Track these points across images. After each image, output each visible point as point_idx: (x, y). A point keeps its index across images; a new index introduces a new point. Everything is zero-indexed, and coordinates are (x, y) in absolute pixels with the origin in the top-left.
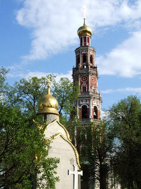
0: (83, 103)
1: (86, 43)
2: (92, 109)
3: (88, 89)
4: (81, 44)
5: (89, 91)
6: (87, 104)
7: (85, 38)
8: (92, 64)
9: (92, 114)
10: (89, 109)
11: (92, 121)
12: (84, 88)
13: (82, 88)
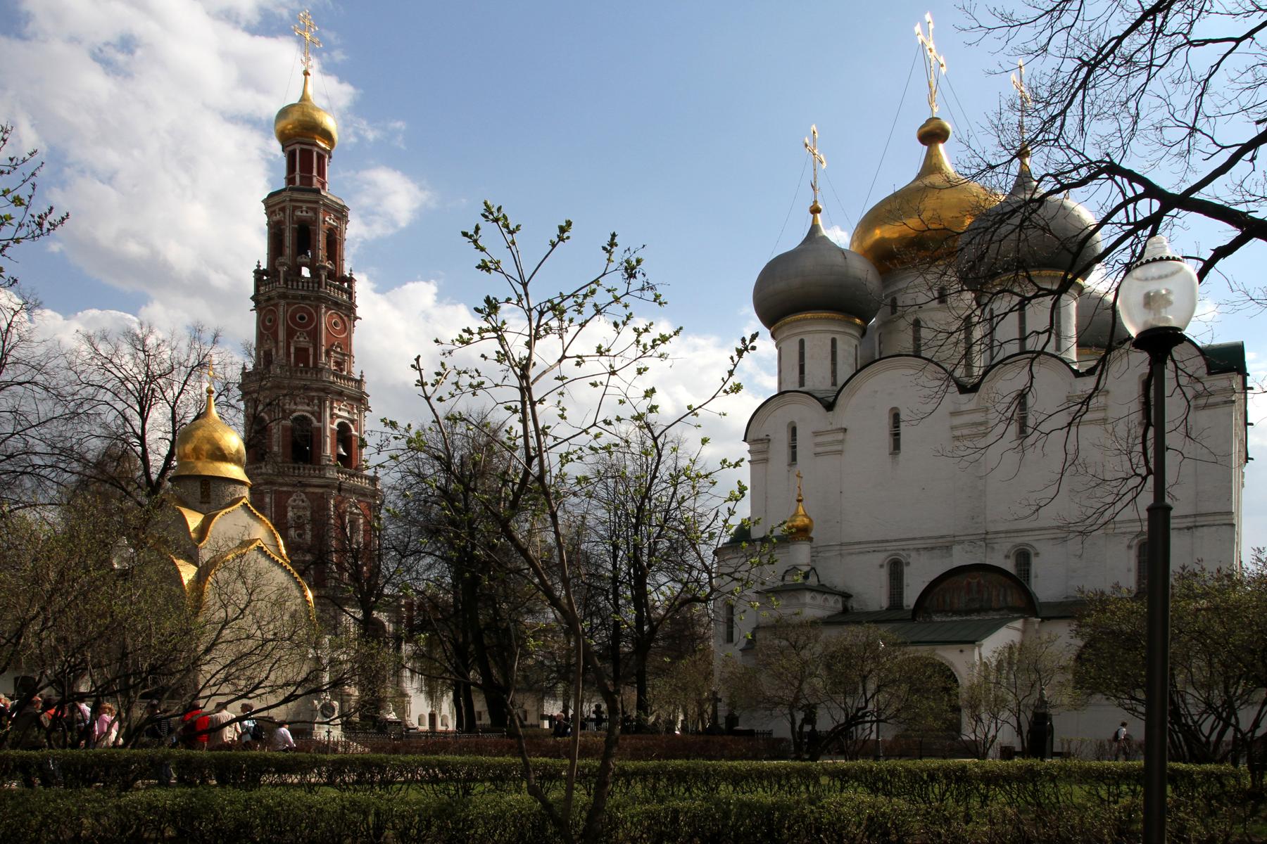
0: (302, 410)
1: (311, 179)
2: (332, 429)
3: (317, 356)
4: (290, 180)
5: (320, 365)
6: (313, 413)
7: (306, 155)
8: (335, 262)
9: (329, 449)
10: (320, 432)
11: (331, 474)
12: (302, 354)
13: (292, 350)
